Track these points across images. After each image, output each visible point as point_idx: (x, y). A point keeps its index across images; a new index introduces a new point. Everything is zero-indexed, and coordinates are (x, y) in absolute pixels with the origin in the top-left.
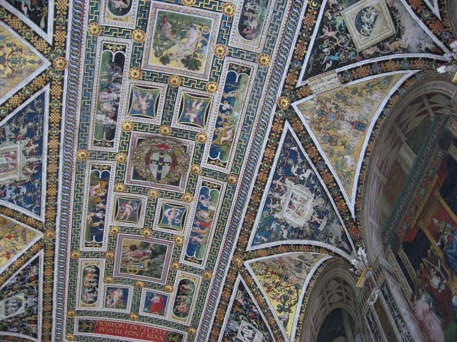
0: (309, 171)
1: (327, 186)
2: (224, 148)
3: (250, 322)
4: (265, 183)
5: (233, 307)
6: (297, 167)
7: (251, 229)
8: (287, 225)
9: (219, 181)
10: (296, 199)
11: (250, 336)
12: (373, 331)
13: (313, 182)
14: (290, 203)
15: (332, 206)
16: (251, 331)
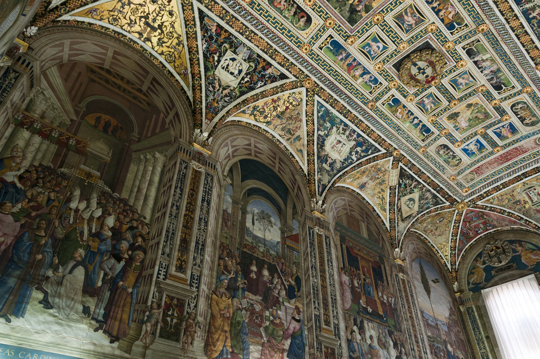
0: (355, 159)
1: (346, 172)
2: (394, 108)
3: (247, 74)
4: (358, 127)
5: (265, 60)
6: (360, 152)
7: (331, 105)
8: (327, 136)
9: (375, 95)
10: (342, 147)
11: (231, 69)
12: (310, 239)
13: (349, 161)
14: (340, 142)
15: (336, 174)
16: (236, 72)
